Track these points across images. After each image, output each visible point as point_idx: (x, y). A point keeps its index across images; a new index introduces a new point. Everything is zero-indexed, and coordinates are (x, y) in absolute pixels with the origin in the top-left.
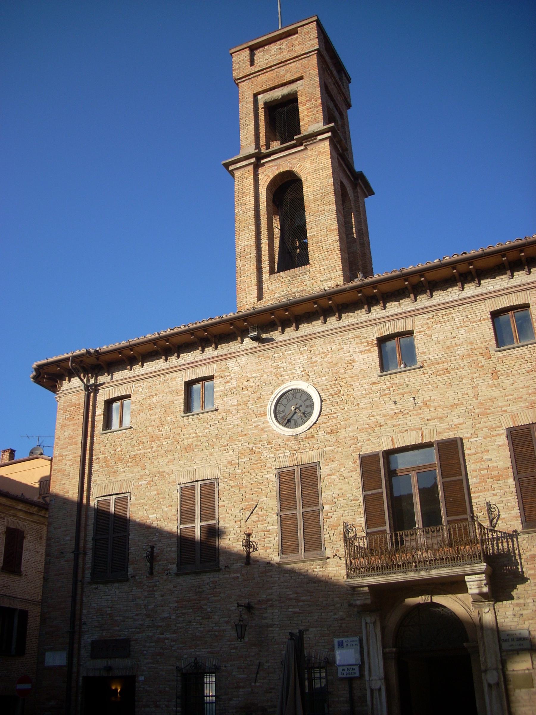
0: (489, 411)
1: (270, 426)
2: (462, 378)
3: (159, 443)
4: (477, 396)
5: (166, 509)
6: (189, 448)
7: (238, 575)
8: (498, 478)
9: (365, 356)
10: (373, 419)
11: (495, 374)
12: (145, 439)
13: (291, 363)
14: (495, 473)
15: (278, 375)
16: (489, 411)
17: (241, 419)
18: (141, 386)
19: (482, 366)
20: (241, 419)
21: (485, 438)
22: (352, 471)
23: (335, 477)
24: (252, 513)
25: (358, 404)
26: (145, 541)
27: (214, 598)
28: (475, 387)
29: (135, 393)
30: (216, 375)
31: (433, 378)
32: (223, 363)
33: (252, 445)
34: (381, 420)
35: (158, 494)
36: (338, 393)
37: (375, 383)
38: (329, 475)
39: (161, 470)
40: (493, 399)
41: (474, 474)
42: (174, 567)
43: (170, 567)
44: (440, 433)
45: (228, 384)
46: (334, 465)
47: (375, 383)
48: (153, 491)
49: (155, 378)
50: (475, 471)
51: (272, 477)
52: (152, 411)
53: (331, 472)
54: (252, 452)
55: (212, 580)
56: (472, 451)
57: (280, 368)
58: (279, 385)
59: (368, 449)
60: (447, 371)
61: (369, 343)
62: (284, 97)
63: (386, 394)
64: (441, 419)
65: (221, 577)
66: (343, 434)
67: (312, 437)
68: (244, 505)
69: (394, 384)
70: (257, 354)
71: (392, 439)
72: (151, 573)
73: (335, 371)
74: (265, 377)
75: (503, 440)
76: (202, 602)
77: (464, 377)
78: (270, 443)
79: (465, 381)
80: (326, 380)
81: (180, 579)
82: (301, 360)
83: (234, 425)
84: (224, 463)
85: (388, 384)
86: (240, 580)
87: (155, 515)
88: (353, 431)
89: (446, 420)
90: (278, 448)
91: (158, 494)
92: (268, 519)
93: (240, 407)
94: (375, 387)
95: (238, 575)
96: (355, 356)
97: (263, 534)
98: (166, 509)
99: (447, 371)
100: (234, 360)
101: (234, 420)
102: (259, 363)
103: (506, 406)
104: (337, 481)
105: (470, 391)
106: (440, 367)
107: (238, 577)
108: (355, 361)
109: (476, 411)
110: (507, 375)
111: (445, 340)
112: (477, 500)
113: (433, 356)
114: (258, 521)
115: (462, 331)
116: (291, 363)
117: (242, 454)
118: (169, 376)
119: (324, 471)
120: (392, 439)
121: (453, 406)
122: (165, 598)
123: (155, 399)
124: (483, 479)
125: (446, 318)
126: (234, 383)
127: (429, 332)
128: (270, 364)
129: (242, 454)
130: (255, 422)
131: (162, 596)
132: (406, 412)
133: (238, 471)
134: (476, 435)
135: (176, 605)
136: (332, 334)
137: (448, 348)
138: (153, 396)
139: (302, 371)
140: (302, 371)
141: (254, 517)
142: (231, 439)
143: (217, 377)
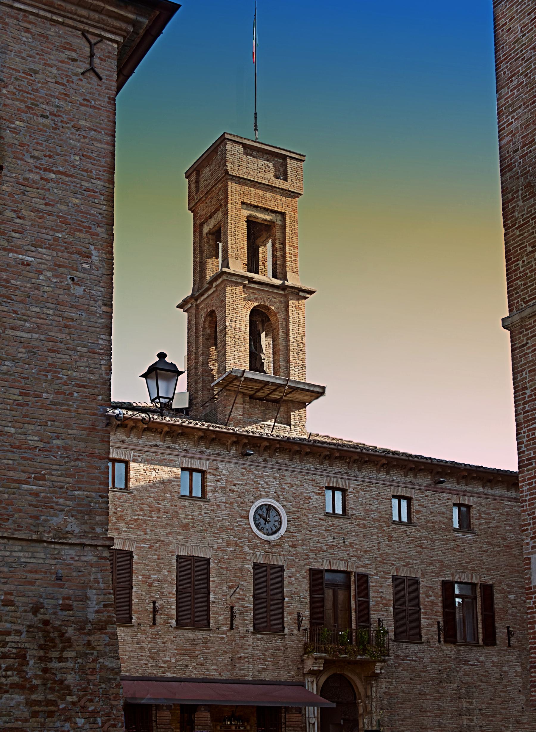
0: (385, 561)
2: (373, 534)
3: (158, 515)
4: (379, 549)
6: (186, 527)
7: (225, 636)
8: (385, 605)
9: (318, 497)
10: (319, 545)
11: (390, 539)
12: (146, 508)
13: (267, 483)
14: (384, 601)
15: (257, 489)
16: (385, 561)
17: (228, 515)
18: (139, 456)
19: (384, 530)
20: (228, 515)
21: (381, 578)
22: (304, 578)
23: (293, 579)
24: (235, 592)
25: (310, 531)
26: (148, 596)
27: (206, 651)
28: (379, 543)
30: (209, 471)
31: (357, 528)
32: (215, 463)
33: (236, 539)
34: (325, 548)
35: (158, 559)
36: (298, 518)
38: (289, 577)
39: (162, 539)
40: (387, 554)
41: (374, 599)
42: (174, 621)
43: (170, 621)
44: (357, 567)
45: (218, 483)
46: (293, 570)
47: (322, 520)
48: (155, 555)
50: (373, 597)
53: (291, 575)
54: (236, 544)
55: (204, 636)
56: (374, 584)
57: (259, 484)
58: (259, 497)
60: (365, 527)
63: (328, 530)
64: (359, 558)
65: (211, 635)
66: (300, 549)
67: (280, 546)
68: (230, 584)
69: (333, 524)
71: (330, 563)
72: (154, 623)
73: (297, 501)
75: (390, 582)
76: (197, 652)
77: (374, 534)
78: (249, 541)
79: (374, 537)
80: (291, 505)
81: (178, 632)
83: (223, 519)
84: (215, 547)
85: (330, 523)
86: (226, 640)
88: (306, 550)
89: (362, 559)
90: (255, 547)
91: (158, 559)
92: (247, 599)
93: (227, 505)
94: (323, 523)
95: (225, 636)
96: (311, 495)
97: (242, 609)
98: (167, 573)
99: (365, 527)
101: (223, 514)
103: (395, 561)
104: (294, 582)
105: (376, 544)
106: (361, 522)
107: (224, 638)
108: (310, 498)
110: (397, 541)
111: (366, 504)
112: (373, 616)
113: (358, 513)
114: (240, 599)
115: (376, 502)
116: (267, 483)
117: (229, 544)
120: (330, 563)
121: (366, 552)
122: (166, 645)
124: (378, 603)
127: (357, 495)
128: (252, 477)
129: (229, 544)
130: (240, 521)
131: (164, 643)
132: (339, 546)
133: (226, 557)
134: (376, 574)
135: (176, 651)
136: (297, 472)
139: (275, 493)
141: (237, 595)
142: (220, 529)
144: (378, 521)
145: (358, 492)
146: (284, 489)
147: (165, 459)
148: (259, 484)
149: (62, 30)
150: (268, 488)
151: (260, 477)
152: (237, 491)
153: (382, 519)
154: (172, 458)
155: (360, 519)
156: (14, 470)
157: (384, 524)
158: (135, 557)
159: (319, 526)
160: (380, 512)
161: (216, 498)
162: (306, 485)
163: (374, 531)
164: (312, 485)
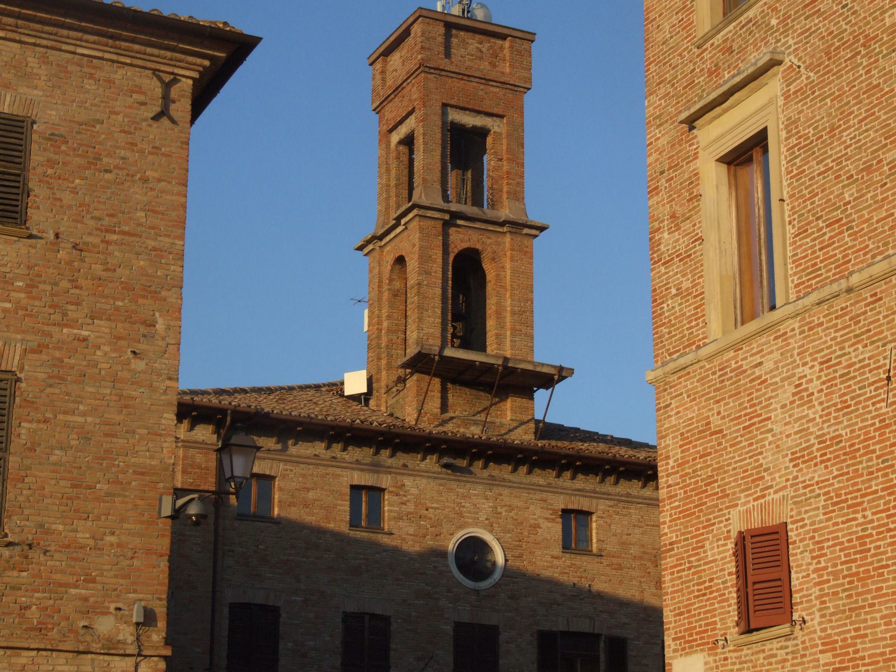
1: (451, 572)
2: (632, 578)
5: (327, 639)
9: (550, 525)
15: (460, 514)
18: (291, 470)
24: (426, 665)
28: (642, 592)
29: (284, 477)
30: (390, 489)
32: (399, 477)
33: (430, 588)
37: (556, 558)
38: (507, 642)
45: (404, 506)
47: (556, 558)
49: (311, 467)
51: (449, 628)
52: (308, 510)
57: (464, 507)
58: (461, 527)
59: (546, 626)
60: (620, 567)
61: (554, 512)
62: (474, 127)
63: (565, 573)
70: (439, 481)
73: (519, 531)
74: (446, 511)
77: (634, 578)
78: (449, 591)
79: (634, 582)
82: (486, 506)
85: (568, 563)
87: (312, 643)
93: (417, 538)
94: (556, 562)
96: (541, 521)
98: (327, 639)
100: (412, 478)
102: (440, 493)
106: (614, 560)
109: (641, 615)
115: (637, 531)
118: (330, 470)
119: (503, 637)
123: (311, 495)
125: (625, 511)
126: (411, 507)
127: (608, 521)
133: (413, 614)
136: (520, 488)
137: (624, 543)
138: (308, 490)
139: (487, 519)
140: (487, 519)
143: (391, 492)
144: (641, 558)
145: (610, 516)
146: (500, 513)
147: (327, 474)
148: (464, 507)
149: (130, 71)
150: (477, 513)
151: (464, 497)
152: (431, 519)
153: (645, 556)
154: (338, 471)
155: (613, 557)
156: (63, 572)
157: (649, 564)
158: (284, 615)
159: (551, 567)
160: (643, 546)
161: (400, 528)
162: (532, 508)
163: (634, 573)
164: (542, 508)
